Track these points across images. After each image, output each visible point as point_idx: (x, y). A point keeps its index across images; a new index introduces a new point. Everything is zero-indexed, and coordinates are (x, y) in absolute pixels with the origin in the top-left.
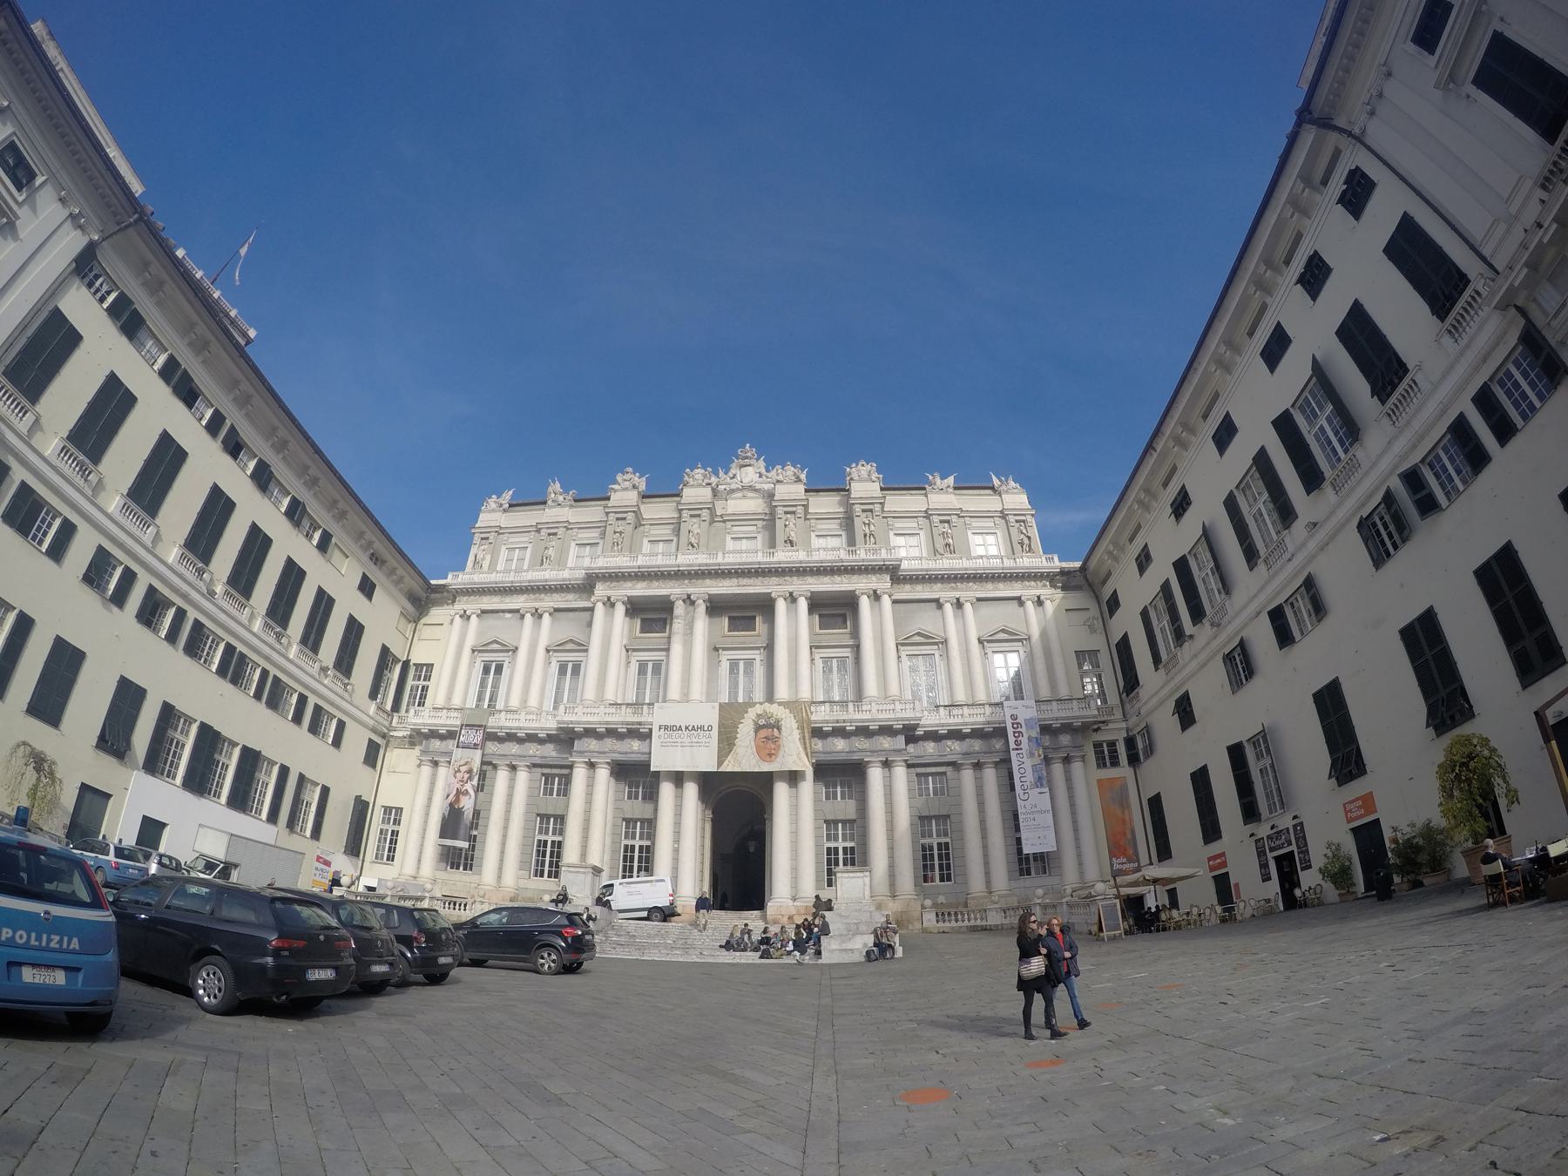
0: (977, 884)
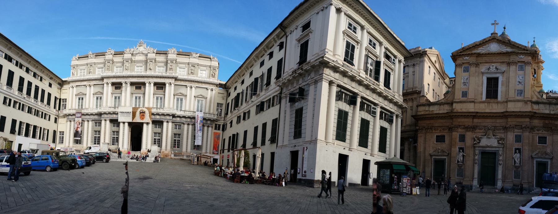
0: (184, 149)
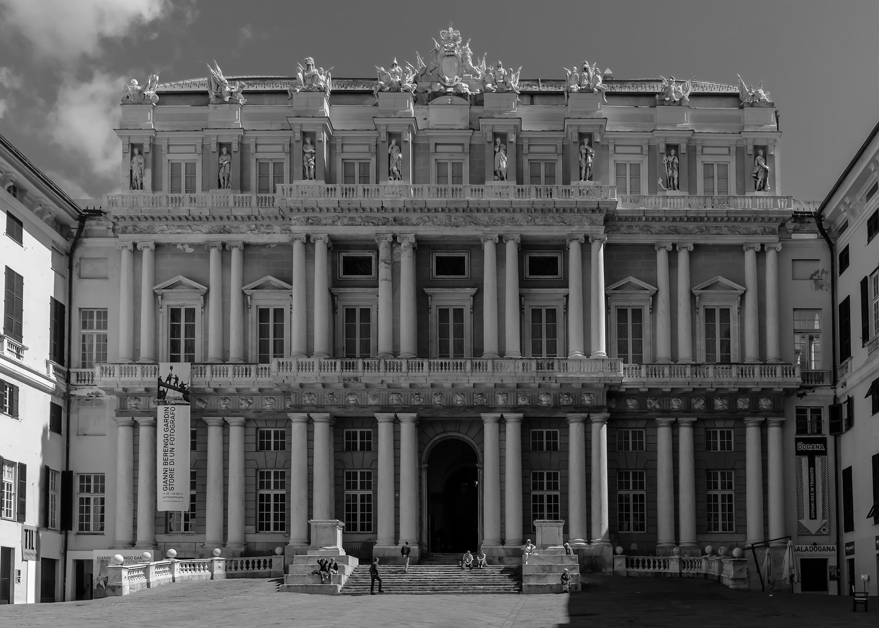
0: (664, 534)
